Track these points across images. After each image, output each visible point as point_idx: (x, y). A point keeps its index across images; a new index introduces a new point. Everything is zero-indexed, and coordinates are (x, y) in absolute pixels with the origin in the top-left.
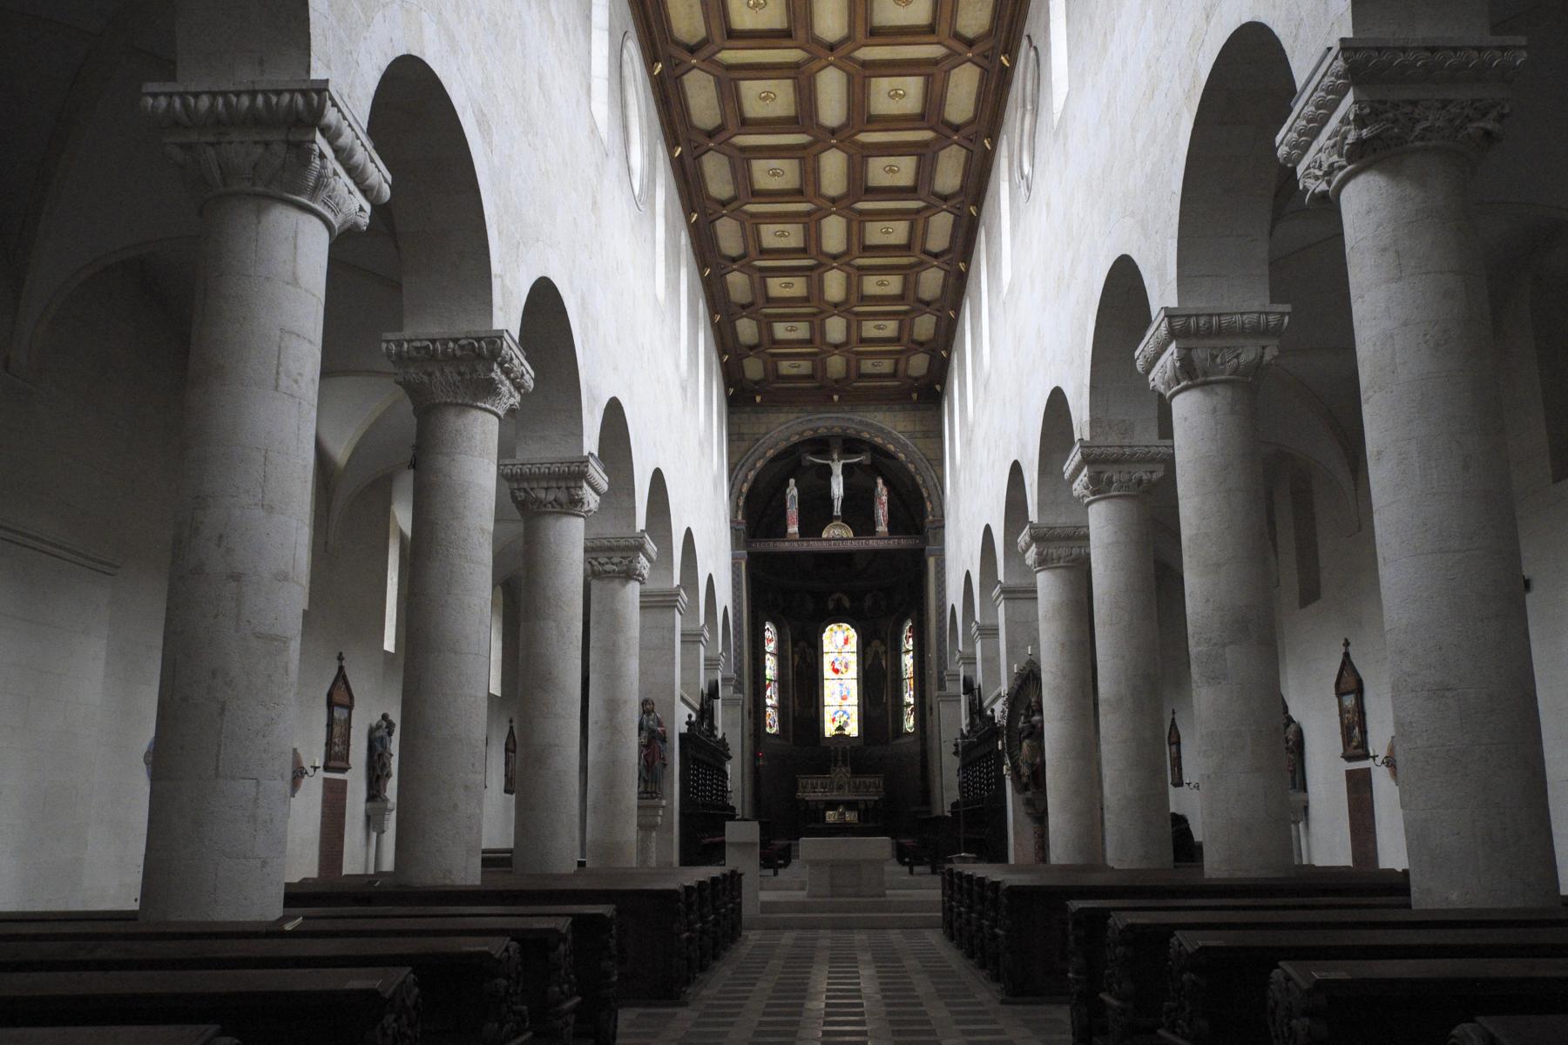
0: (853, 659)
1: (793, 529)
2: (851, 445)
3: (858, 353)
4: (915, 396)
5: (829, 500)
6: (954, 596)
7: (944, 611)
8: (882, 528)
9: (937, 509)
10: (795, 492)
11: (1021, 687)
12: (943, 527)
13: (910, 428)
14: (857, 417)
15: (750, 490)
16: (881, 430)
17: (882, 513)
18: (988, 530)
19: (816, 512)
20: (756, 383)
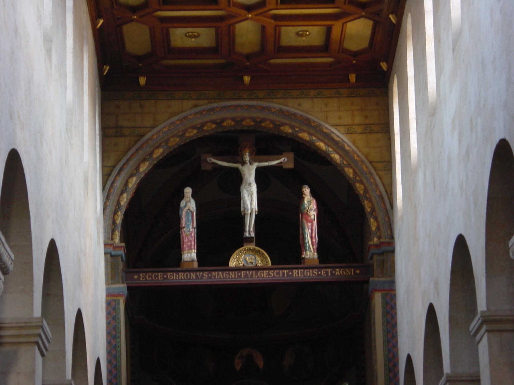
1: (190, 255)
2: (267, 143)
3: (276, 17)
4: (353, 78)
5: (241, 219)
6: (411, 341)
7: (396, 365)
8: (310, 253)
10: (192, 205)
12: (393, 251)
13: (347, 120)
14: (275, 105)
15: (132, 203)
16: (307, 122)
17: (310, 233)
18: (461, 243)
19: (221, 233)
20: (140, 58)
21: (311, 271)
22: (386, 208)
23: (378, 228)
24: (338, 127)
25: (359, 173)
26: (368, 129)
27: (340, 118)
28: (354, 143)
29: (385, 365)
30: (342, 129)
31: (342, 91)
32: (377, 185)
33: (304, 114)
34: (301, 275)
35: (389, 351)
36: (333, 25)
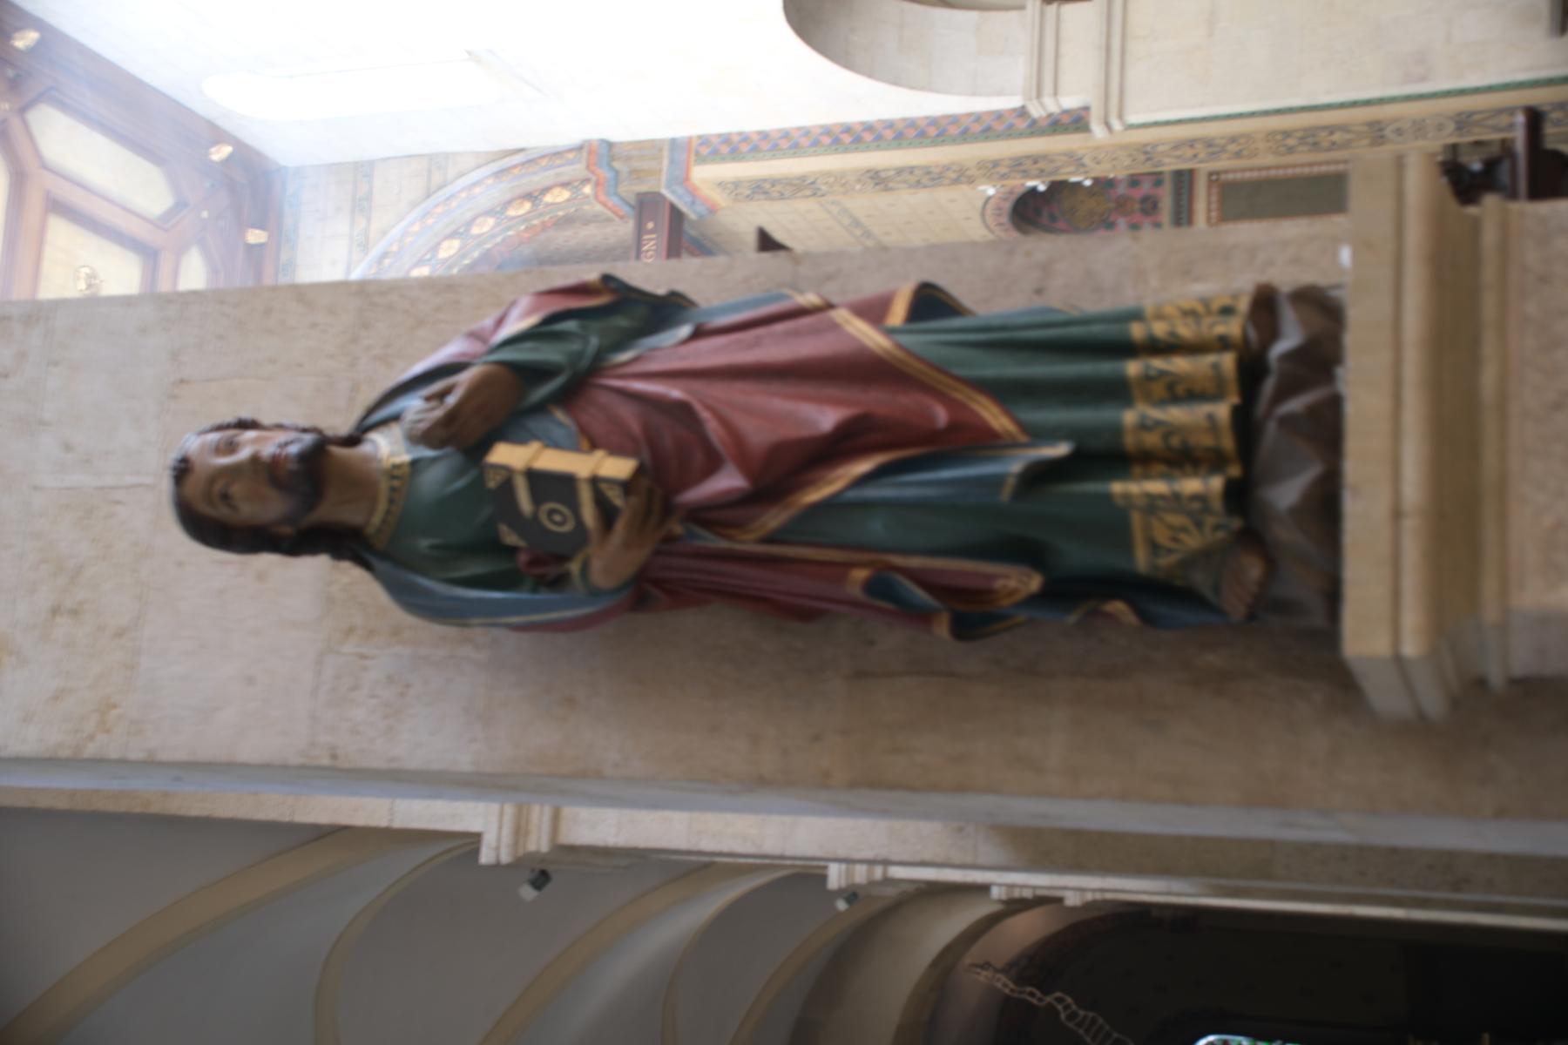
4: (255, 236)
9: (577, 169)
12: (610, 145)
22: (523, 164)
23: (565, 185)
28: (384, 233)
29: (846, 151)
31: (284, 258)
32: (475, 184)
35: (816, 143)
36: (48, 192)
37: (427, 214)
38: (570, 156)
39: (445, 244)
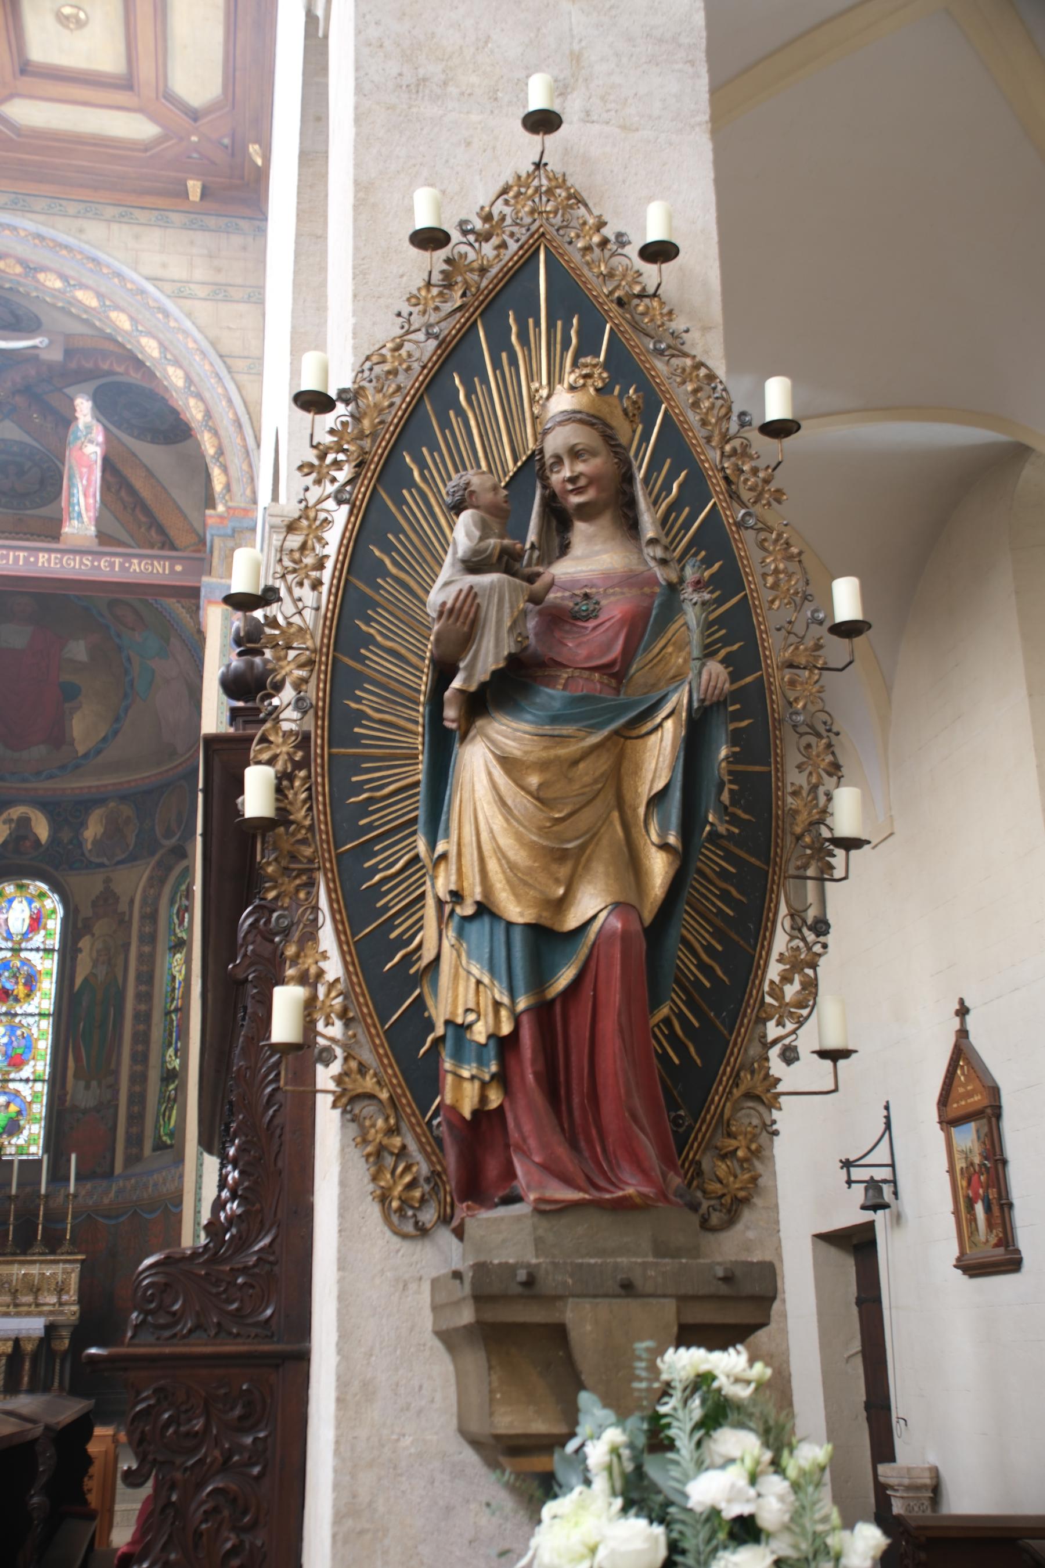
0: (48, 966)
4: (194, 188)
11: (455, 355)
14: (27, 224)
21: (78, 558)
23: (228, 487)
24: (159, 283)
25: (196, 379)
26: (220, 292)
27: (164, 266)
28: (189, 315)
30: (168, 287)
31: (175, 217)
32: (230, 401)
33: (86, 247)
34: (56, 564)
37: (203, 354)
38: (248, 492)
39: (180, 373)
